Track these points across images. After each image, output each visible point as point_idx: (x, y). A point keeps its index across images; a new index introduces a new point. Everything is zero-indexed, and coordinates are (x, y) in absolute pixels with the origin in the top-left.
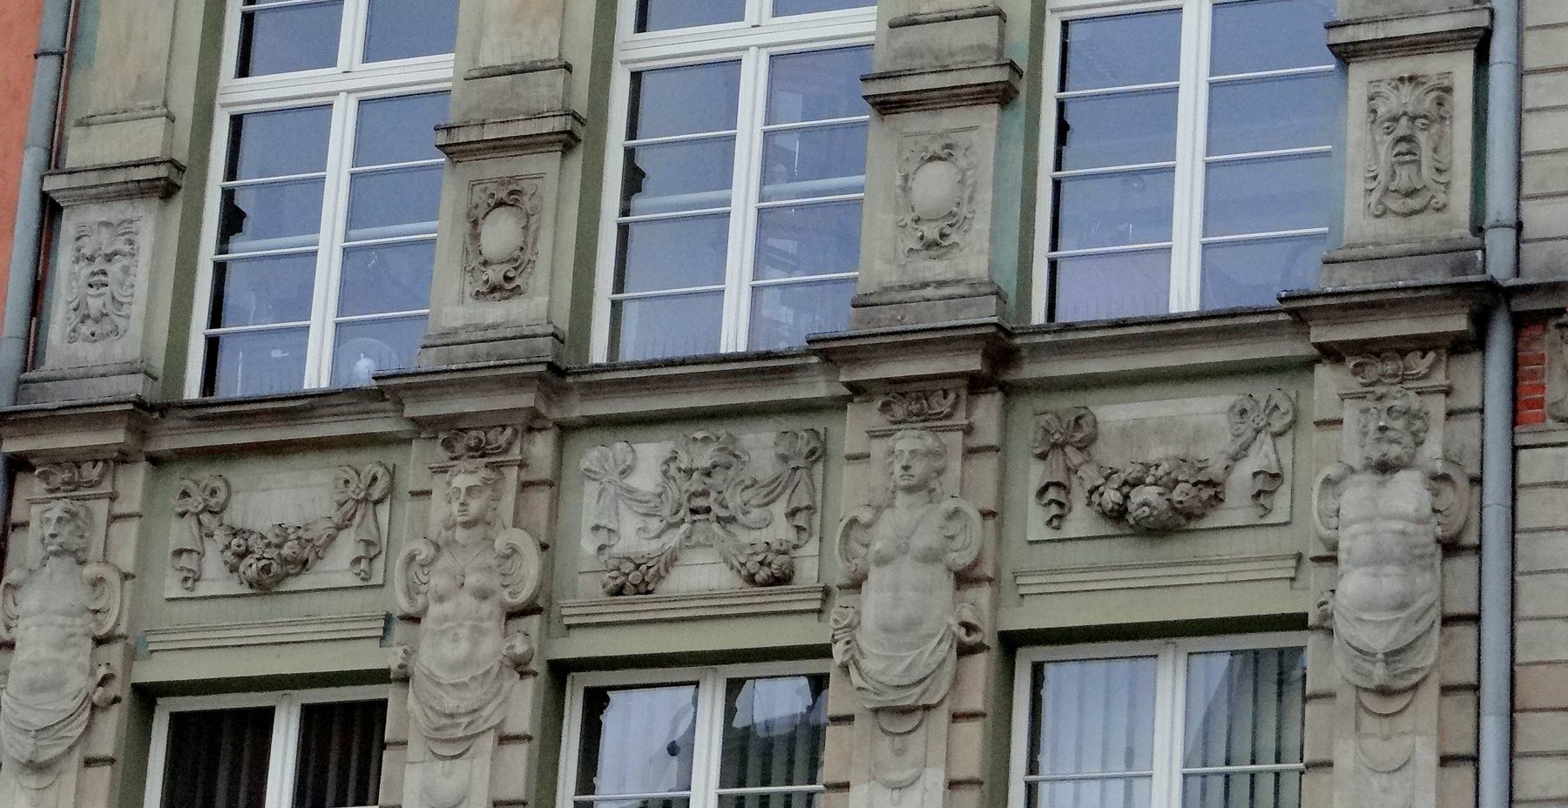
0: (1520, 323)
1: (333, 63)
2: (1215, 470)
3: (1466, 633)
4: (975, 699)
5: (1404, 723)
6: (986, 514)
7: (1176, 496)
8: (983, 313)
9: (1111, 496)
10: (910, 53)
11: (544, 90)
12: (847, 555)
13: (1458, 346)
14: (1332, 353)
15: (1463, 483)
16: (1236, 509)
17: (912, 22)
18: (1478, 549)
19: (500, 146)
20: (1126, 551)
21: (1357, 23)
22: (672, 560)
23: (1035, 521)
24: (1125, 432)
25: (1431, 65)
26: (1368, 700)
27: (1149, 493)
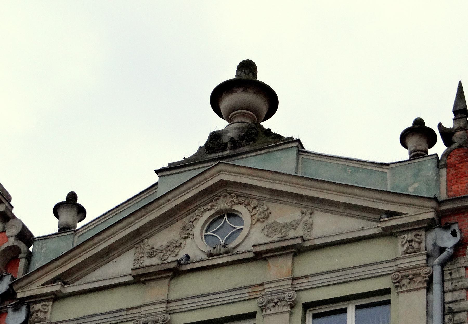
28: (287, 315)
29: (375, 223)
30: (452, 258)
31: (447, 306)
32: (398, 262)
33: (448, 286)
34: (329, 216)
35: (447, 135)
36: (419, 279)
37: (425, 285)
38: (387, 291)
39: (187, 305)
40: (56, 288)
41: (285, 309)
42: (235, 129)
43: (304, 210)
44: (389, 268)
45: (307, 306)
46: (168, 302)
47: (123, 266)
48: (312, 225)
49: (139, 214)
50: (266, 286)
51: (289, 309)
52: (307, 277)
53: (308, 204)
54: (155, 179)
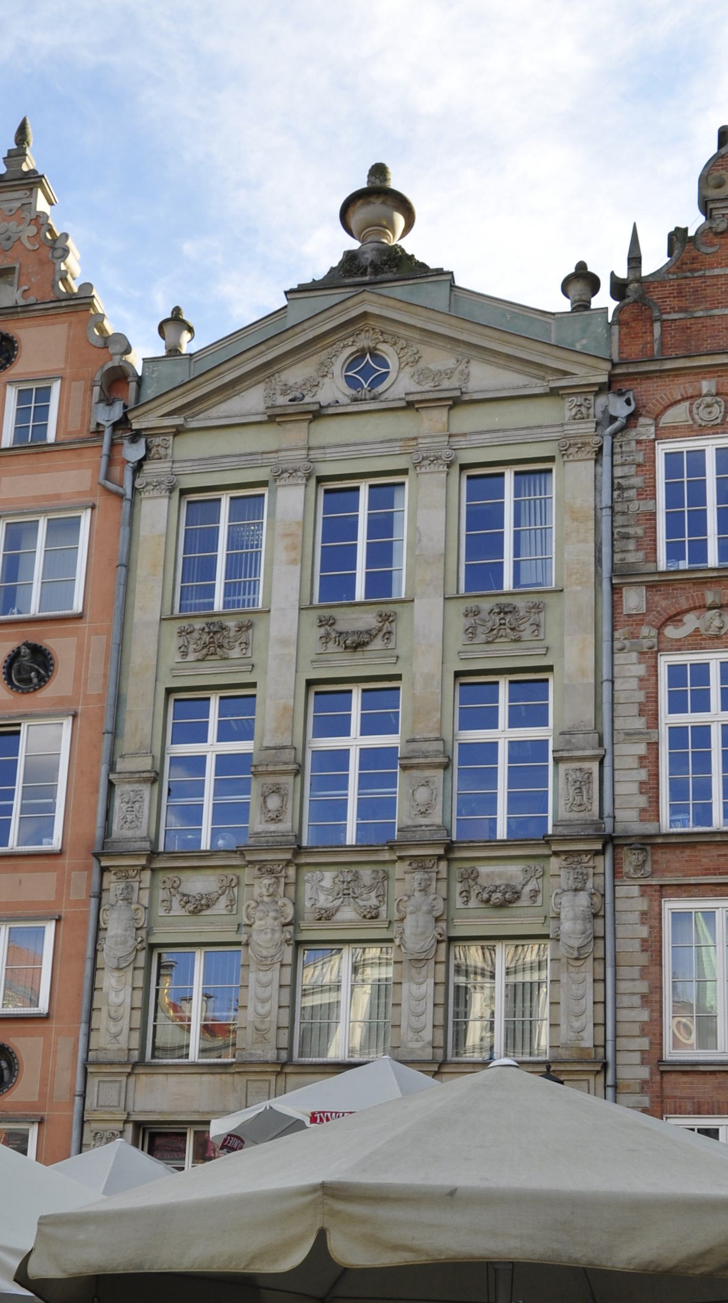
0: (615, 847)
1: (206, 741)
2: (519, 888)
3: (600, 943)
4: (442, 958)
5: (583, 969)
6: (444, 899)
7: (507, 896)
8: (442, 835)
9: (485, 896)
10: (413, 751)
11: (288, 755)
12: (398, 911)
13: (597, 853)
14: (556, 854)
15: (600, 896)
16: (524, 901)
17: (414, 740)
18: (604, 917)
19: (273, 773)
20: (492, 912)
21: (563, 750)
22: (337, 910)
23: (459, 902)
24: (488, 875)
25: (586, 765)
26: (571, 962)
27: (499, 895)
28: (444, 475)
29: (540, 381)
30: (623, 429)
31: (616, 481)
32: (565, 427)
33: (618, 459)
34: (487, 367)
35: (619, 288)
36: (588, 448)
37: (594, 456)
38: (551, 459)
39: (330, 454)
40: (177, 421)
41: (441, 468)
42: (373, 250)
43: (460, 358)
44: (554, 433)
45: (463, 467)
46: (309, 449)
47: (252, 401)
48: (468, 375)
49: (272, 342)
50: (420, 441)
51: (445, 469)
52: (465, 435)
53: (464, 351)
54: (285, 302)
